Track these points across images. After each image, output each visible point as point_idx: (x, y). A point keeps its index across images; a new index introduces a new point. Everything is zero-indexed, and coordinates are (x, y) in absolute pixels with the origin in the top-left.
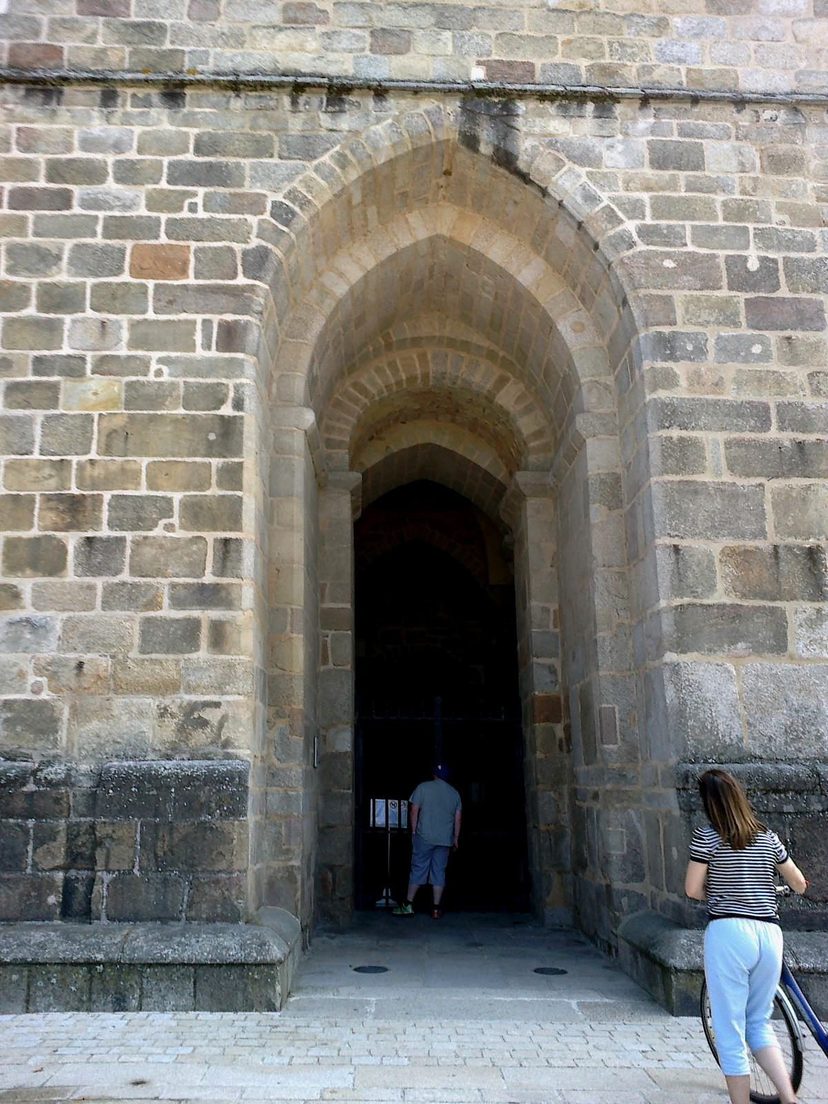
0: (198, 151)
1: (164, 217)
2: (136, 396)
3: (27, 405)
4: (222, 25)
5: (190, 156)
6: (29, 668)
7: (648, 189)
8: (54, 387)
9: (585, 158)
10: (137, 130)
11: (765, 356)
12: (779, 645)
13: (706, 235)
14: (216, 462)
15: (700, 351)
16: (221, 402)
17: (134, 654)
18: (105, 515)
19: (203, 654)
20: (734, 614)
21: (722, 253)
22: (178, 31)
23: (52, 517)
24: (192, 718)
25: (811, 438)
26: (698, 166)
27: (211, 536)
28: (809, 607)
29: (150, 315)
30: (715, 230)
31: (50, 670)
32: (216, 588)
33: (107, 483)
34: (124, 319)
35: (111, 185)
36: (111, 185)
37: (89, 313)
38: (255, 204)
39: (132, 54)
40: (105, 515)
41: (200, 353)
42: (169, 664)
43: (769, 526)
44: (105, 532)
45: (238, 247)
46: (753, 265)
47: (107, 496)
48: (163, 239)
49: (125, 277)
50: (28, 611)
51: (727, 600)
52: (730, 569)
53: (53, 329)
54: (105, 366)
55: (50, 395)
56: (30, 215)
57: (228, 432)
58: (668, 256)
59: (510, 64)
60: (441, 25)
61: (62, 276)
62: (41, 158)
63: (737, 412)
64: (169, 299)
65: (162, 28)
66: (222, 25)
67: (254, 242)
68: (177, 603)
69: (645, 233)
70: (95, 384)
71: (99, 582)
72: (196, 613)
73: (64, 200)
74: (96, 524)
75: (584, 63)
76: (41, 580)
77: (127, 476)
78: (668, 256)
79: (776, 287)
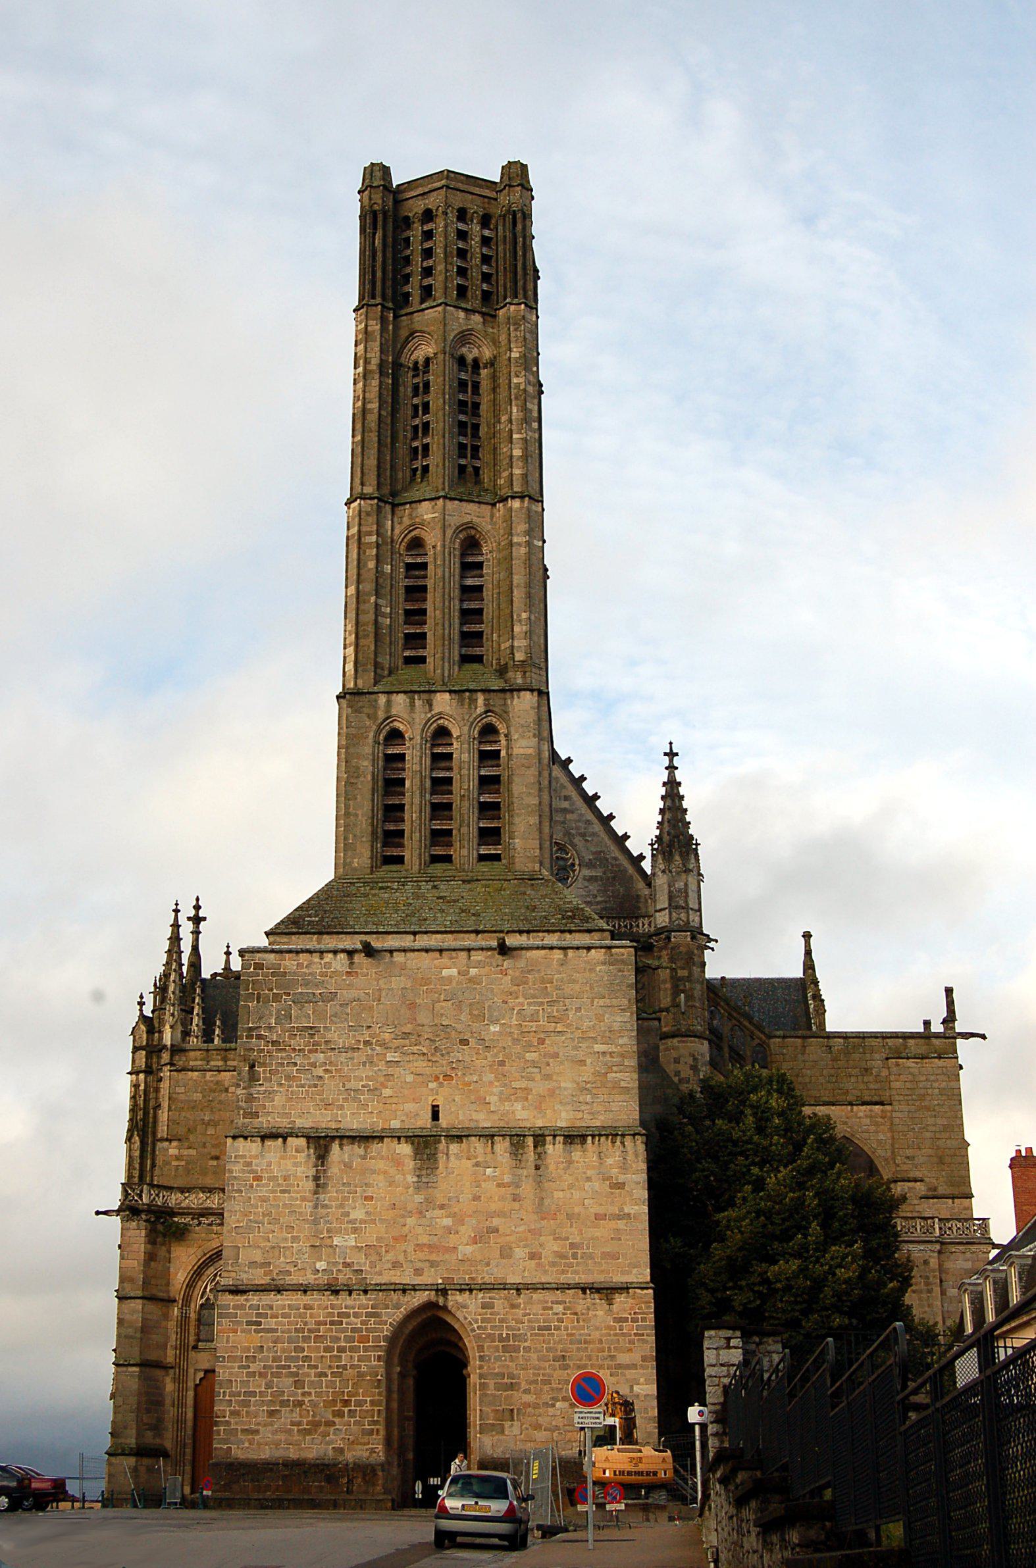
5: (370, 1310)
9: (465, 1307)
11: (505, 1360)
12: (503, 1432)
13: (493, 1328)
15: (490, 1359)
27: (376, 1408)
33: (353, 1396)
34: (356, 1355)
46: (504, 1336)
60: (432, 1267)
62: (336, 1312)
63: (497, 1374)
64: (366, 1349)
66: (377, 1269)
75: (467, 1277)
77: (357, 1394)
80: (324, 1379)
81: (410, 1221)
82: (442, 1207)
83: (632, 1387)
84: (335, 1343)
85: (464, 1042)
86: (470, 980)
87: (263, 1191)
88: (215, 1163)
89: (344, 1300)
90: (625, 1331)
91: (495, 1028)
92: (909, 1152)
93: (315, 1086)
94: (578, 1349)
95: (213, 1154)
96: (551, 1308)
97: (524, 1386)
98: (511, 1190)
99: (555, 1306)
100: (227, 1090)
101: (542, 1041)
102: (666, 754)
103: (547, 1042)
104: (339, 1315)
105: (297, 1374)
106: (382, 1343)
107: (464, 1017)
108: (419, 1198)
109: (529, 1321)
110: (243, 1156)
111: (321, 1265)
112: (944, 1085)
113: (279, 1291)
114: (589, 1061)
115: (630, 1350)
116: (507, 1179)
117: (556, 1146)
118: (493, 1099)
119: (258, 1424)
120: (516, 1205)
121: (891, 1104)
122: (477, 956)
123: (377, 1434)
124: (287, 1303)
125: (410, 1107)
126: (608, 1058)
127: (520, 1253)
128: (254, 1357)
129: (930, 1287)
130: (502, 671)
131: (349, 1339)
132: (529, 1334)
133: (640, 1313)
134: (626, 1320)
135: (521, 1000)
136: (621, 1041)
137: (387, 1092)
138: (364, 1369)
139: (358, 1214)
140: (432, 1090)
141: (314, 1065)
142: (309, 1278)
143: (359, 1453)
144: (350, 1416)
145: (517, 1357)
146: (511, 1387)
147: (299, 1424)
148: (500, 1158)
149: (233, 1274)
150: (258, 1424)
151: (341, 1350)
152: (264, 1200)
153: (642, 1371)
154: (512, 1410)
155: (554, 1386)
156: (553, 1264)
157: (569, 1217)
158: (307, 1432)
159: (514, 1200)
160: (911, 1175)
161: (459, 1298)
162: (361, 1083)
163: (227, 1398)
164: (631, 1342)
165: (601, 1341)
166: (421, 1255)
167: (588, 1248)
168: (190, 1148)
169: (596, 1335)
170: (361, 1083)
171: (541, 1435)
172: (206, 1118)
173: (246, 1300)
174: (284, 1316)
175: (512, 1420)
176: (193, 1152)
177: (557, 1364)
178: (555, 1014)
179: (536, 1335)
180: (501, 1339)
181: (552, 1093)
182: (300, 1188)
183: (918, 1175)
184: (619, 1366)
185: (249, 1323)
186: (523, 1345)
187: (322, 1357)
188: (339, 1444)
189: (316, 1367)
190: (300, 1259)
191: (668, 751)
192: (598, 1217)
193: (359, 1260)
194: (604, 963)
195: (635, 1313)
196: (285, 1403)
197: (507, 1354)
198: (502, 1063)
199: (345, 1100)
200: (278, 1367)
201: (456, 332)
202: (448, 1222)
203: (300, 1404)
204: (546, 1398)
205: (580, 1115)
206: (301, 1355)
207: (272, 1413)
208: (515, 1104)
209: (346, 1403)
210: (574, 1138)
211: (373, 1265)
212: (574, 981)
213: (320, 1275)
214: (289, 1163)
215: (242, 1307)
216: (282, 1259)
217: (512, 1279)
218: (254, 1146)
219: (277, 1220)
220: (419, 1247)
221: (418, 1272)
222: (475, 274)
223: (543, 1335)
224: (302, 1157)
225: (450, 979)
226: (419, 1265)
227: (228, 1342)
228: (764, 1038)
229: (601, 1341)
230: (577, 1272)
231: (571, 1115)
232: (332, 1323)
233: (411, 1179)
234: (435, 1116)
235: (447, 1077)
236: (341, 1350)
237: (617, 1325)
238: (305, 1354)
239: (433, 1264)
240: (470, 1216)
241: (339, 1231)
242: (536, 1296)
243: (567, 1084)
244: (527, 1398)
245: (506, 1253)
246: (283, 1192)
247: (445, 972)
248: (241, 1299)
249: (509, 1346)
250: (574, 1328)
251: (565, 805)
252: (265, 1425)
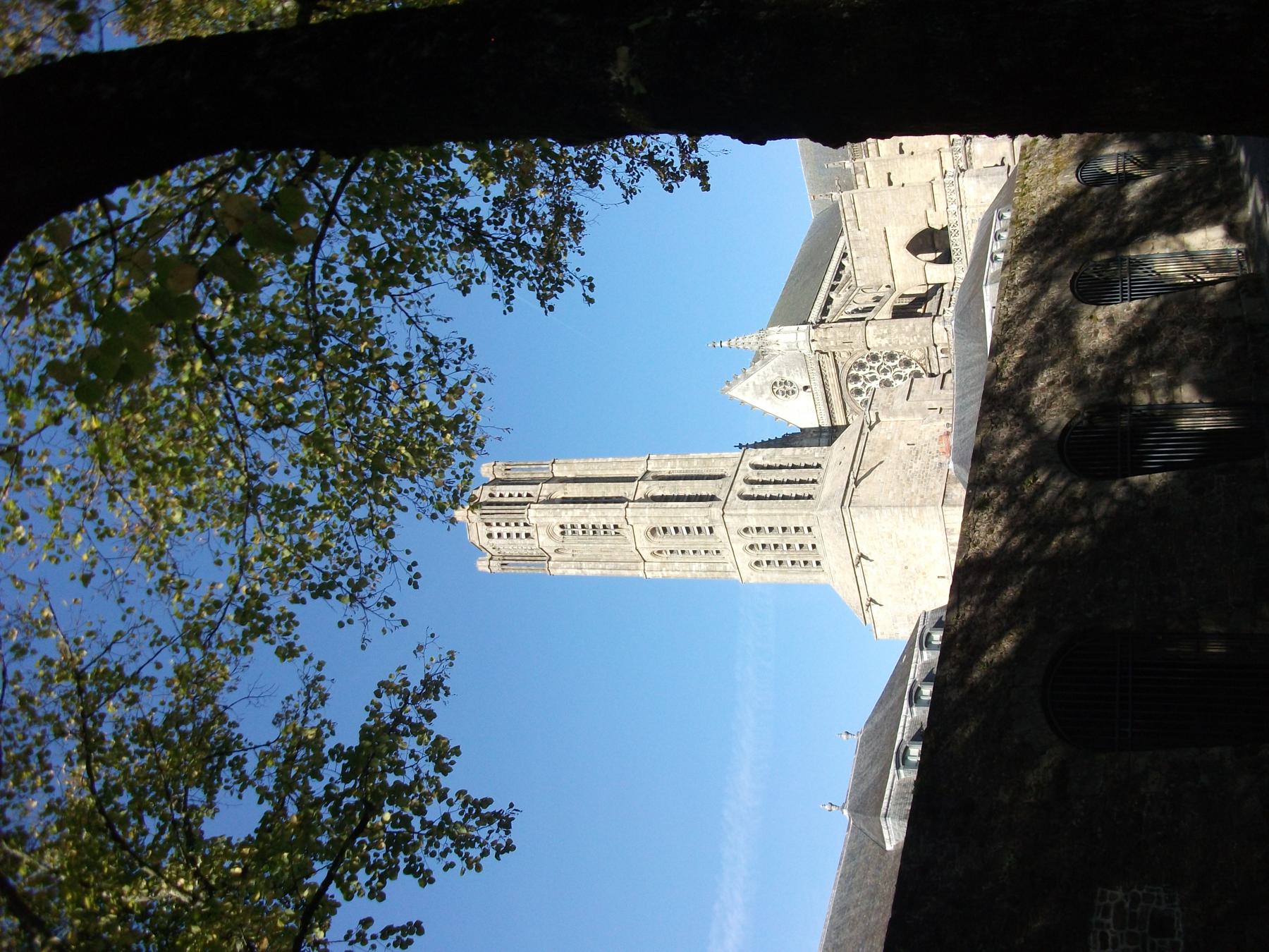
85: (906, 568)
92: (911, 218)
160: (924, 216)
198: (914, 555)
251: (751, 386)
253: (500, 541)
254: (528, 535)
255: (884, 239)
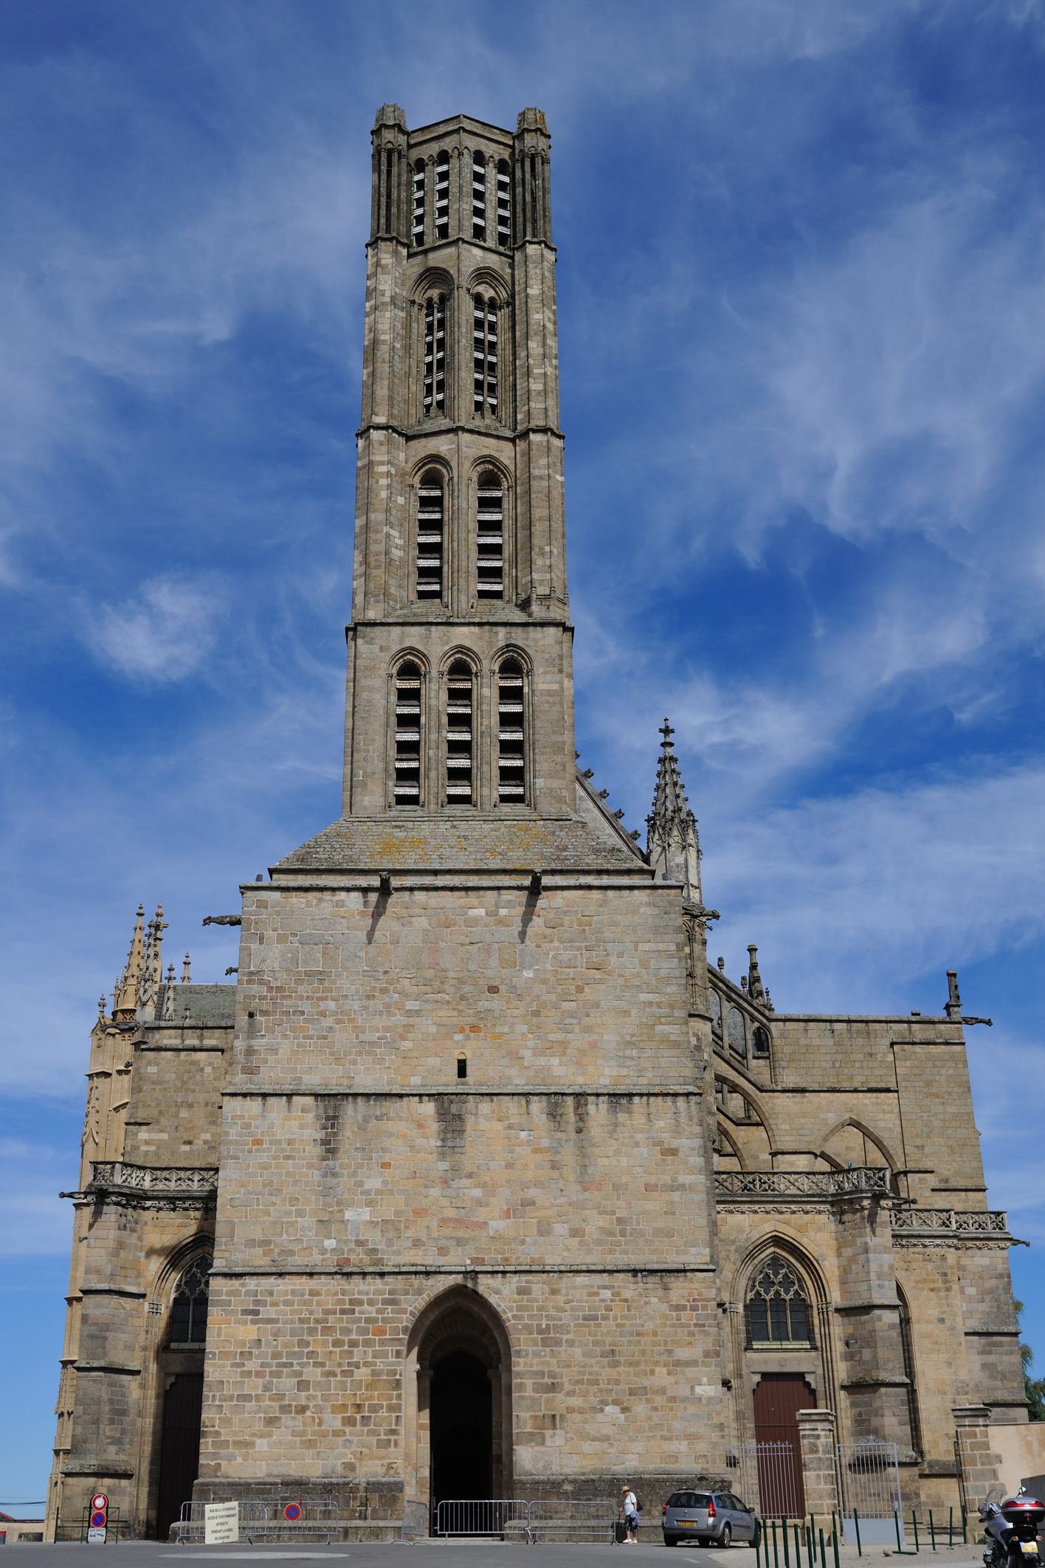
0: (389, 1294)
1: (380, 1316)
2: (374, 1373)
3: (346, 1377)
4: (395, 1248)
5: (387, 1296)
6: (348, 1453)
7: (515, 1302)
8: (353, 1371)
9: (498, 1292)
10: (372, 1287)
11: (545, 1356)
12: (543, 1443)
14: (395, 1393)
15: (527, 1355)
16: (396, 1374)
17: (375, 1449)
18: (366, 1409)
19: (392, 1449)
20: (532, 1434)
21: (535, 1323)
22: (382, 1250)
23: (353, 1410)
24: (390, 1467)
25: (556, 1381)
26: (530, 1294)
27: (394, 1415)
28: (551, 1432)
29: (377, 1348)
30: (534, 1315)
31: (353, 1453)
32: (395, 1430)
33: (367, 1400)
34: (370, 1350)
35: (366, 1307)
36: (366, 1307)
37: (361, 1348)
38: (405, 1311)
39: (370, 1259)
40: (366, 1409)
41: (390, 1359)
42: (383, 1452)
43: (542, 1408)
44: (367, 1414)
45: (400, 1325)
46: (544, 1326)
47: (367, 1403)
48: (380, 1324)
49: (370, 1336)
50: (348, 1437)
51: (530, 1430)
52: (531, 1421)
53: (352, 1352)
54: (366, 1364)
55: (351, 1373)
56: (345, 1316)
57: (398, 1383)
58: (520, 1324)
59: (478, 1258)
60: (458, 1245)
61: (354, 1337)
62: (347, 1298)
63: (536, 1373)
64: (382, 1343)
65: (378, 1250)
66: (395, 1248)
67: (405, 1324)
68: (385, 1434)
69: (514, 1317)
70: (363, 1369)
71: (365, 1429)
72: (390, 1437)
73: (353, 1312)
74: (364, 1412)
75: (500, 1256)
76: (351, 1428)
77: (371, 1398)
78: (520, 1324)
79: (550, 1333)
80: (332, 1379)
81: (435, 1192)
82: (470, 1176)
83: (692, 1388)
84: (346, 1335)
85: (493, 990)
86: (501, 922)
87: (264, 1158)
88: (187, 1148)
89: (357, 1284)
90: (683, 1321)
91: (528, 974)
92: (918, 1142)
93: (325, 1038)
94: (629, 1342)
95: (186, 1139)
96: (597, 1294)
97: (567, 1387)
98: (548, 1156)
99: (601, 1291)
100: (202, 1070)
101: (580, 990)
102: (661, 730)
103: (586, 990)
104: (351, 1302)
105: (300, 1374)
106: (401, 1336)
107: (494, 962)
108: (444, 1166)
109: (573, 1309)
110: (242, 1117)
111: (330, 1243)
112: (951, 1071)
113: (281, 1275)
114: (634, 1012)
115: (690, 1343)
116: (545, 1143)
117: (600, 1106)
118: (527, 1053)
119: (254, 1435)
120: (555, 1174)
121: (897, 1091)
122: (507, 896)
123: (396, 1445)
124: (290, 1288)
125: (433, 1061)
126: (655, 1009)
127: (560, 1229)
128: (250, 1353)
129: (948, 1285)
130: (525, 605)
131: (363, 1331)
132: (572, 1324)
133: (700, 1300)
134: (684, 1308)
135: (556, 944)
136: (669, 990)
137: (408, 1045)
138: (380, 1365)
139: (373, 1183)
140: (457, 1042)
141: (323, 1014)
142: (314, 1260)
143: (371, 1470)
144: (363, 1425)
145: (559, 1352)
146: (553, 1388)
147: (303, 1434)
148: (537, 1120)
149: (227, 1255)
150: (254, 1435)
151: (353, 1344)
152: (265, 1167)
153: (704, 1369)
154: (554, 1416)
155: (602, 1386)
156: (599, 1242)
157: (616, 1187)
158: (310, 1444)
159: (553, 1168)
160: (922, 1167)
161: (496, 1282)
162: (377, 1035)
163: (217, 1403)
164: (691, 1334)
165: (655, 1334)
166: (448, 1231)
167: (638, 1224)
168: (162, 1131)
169: (649, 1326)
170: (377, 1035)
171: (588, 1447)
172: (179, 1100)
173: (243, 1285)
174: (286, 1303)
175: (554, 1427)
176: (164, 1136)
177: (606, 1360)
178: (595, 960)
179: (581, 1325)
180: (540, 1331)
181: (593, 1045)
182: (306, 1153)
183: (928, 1165)
184: (678, 1363)
185: (245, 1312)
186: (565, 1337)
187: (331, 1352)
188: (349, 1458)
189: (322, 1365)
190: (306, 1236)
191: (663, 727)
192: (649, 1188)
193: (375, 1238)
194: (648, 904)
195: (694, 1300)
196: (285, 1409)
197: (548, 1349)
198: (537, 1013)
199: (359, 1053)
200: (279, 1365)
201: (472, 269)
202: (477, 1192)
203: (302, 1410)
204: (594, 1401)
205: (625, 1072)
206: (306, 1350)
207: (271, 1421)
208: (552, 1059)
209: (358, 1407)
210: (618, 1098)
211: (390, 1243)
212: (616, 924)
213: (328, 1255)
214: (294, 1124)
215: (236, 1293)
216: (285, 1236)
217: (552, 1260)
218: (254, 1105)
219: (279, 1191)
220: (444, 1222)
221: (443, 1251)
222: (490, 214)
223: (589, 1326)
224: (310, 1117)
225: (474, 922)
226: (444, 1243)
227: (219, 1335)
228: (765, 1021)
229: (655, 1334)
230: (626, 1252)
231: (615, 1072)
232: (343, 1312)
233: (435, 1142)
234: (462, 1071)
235: (474, 1029)
236: (353, 1344)
237: (674, 1314)
238: (310, 1349)
239: (460, 1242)
240: (502, 1186)
241: (351, 1204)
242: (581, 1279)
243: (610, 1039)
244: (576, 1401)
245: (544, 1229)
246: (287, 1158)
247: (472, 913)
248: (235, 1283)
249: (548, 1337)
250: (624, 1317)
252: (261, 1437)
253: (468, 176)
254: (479, 232)
255: (873, 1085)
